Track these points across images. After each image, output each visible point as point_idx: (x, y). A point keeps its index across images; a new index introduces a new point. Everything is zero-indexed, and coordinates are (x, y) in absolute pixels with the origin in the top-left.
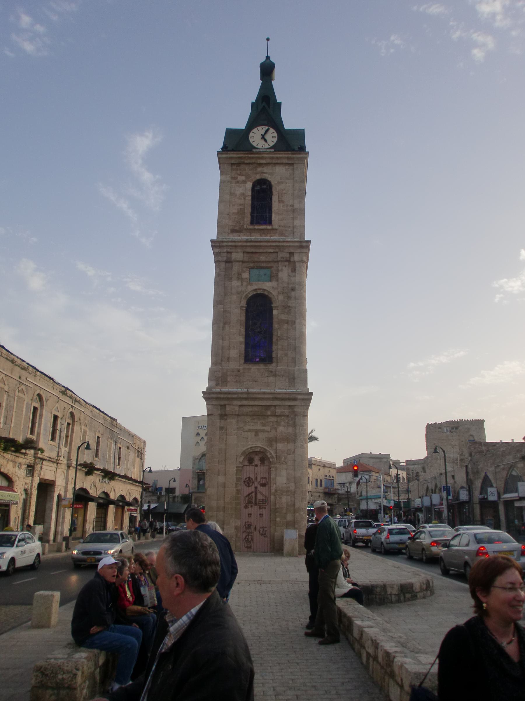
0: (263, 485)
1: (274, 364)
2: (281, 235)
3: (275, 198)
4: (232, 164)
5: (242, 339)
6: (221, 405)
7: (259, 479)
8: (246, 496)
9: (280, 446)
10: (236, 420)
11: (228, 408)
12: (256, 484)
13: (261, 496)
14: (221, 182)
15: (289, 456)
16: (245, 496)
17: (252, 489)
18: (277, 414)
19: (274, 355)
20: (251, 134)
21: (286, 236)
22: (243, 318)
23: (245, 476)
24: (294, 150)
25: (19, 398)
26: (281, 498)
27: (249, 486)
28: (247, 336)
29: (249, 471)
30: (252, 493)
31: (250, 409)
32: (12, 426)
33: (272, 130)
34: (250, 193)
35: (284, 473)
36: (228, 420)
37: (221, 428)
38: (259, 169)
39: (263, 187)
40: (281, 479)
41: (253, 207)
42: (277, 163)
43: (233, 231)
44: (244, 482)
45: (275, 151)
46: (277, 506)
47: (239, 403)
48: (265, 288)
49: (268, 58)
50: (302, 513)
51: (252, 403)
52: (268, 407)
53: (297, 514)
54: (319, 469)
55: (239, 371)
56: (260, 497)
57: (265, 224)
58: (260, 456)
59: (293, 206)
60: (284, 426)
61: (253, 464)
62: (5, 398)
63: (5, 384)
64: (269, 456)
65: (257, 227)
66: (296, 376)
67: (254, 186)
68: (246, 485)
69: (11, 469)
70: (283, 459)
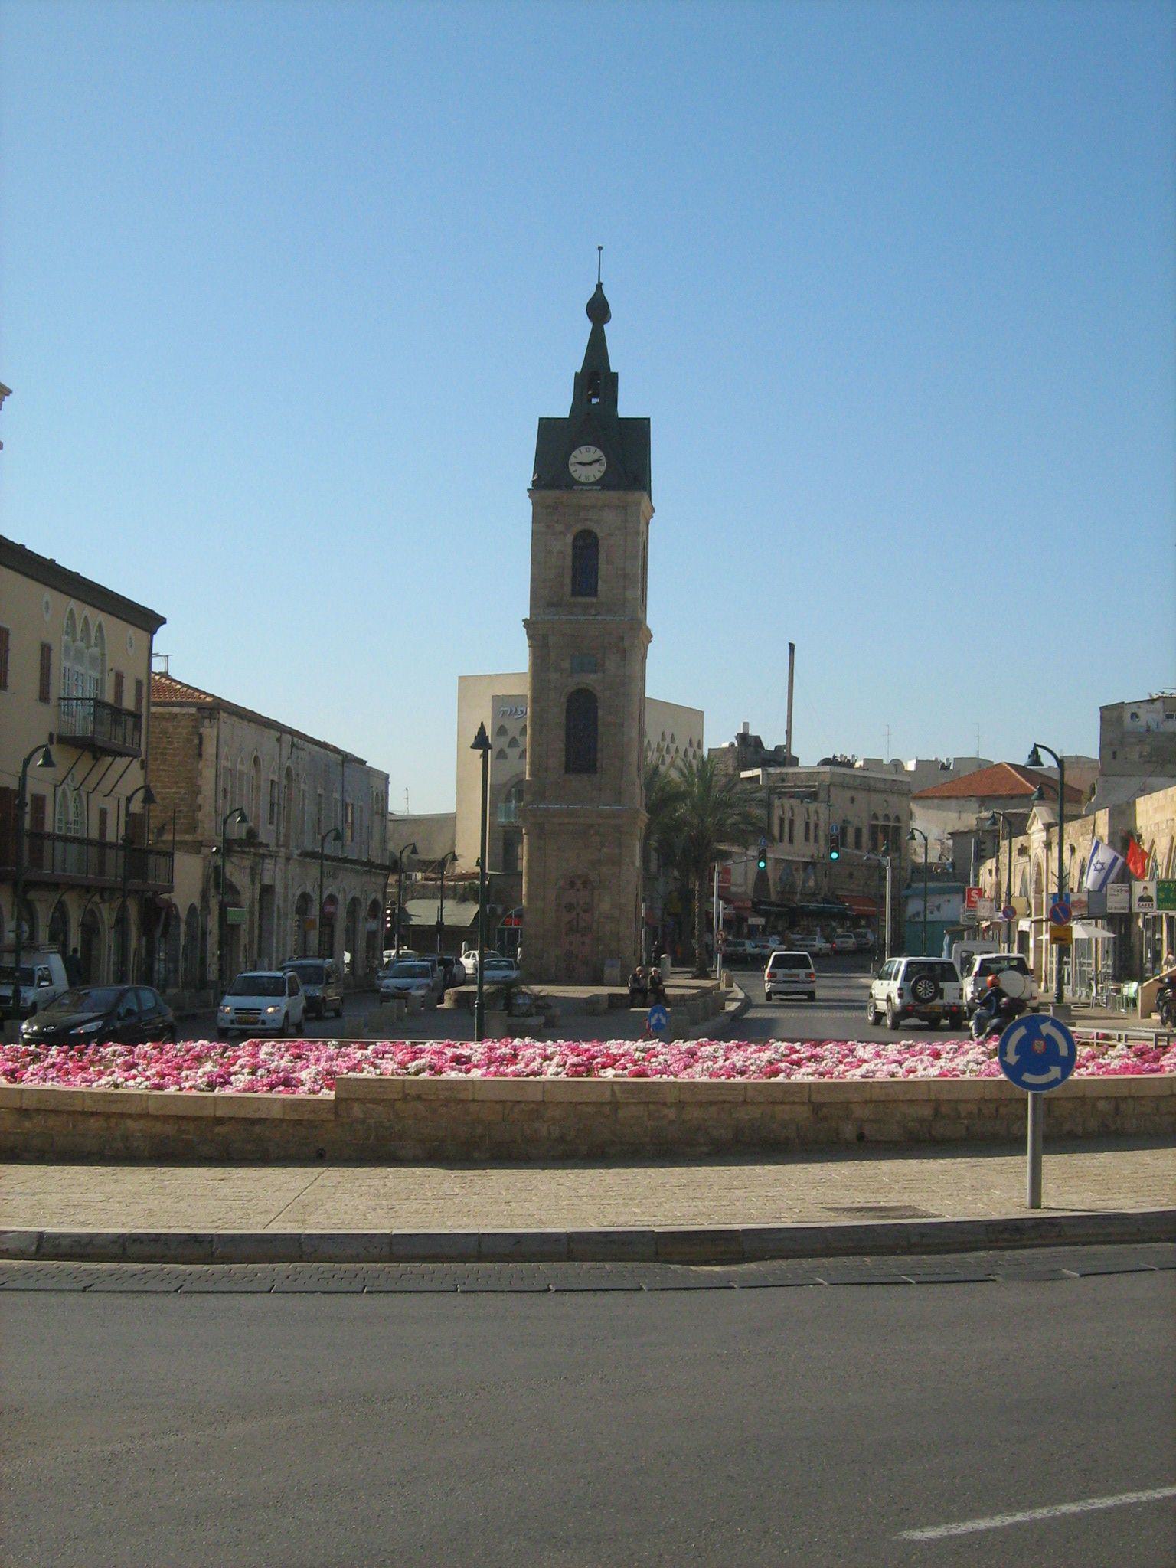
0: (585, 911)
4: (548, 507)
5: (562, 746)
14: (534, 533)
17: (573, 915)
20: (572, 460)
22: (563, 720)
34: (569, 550)
40: (605, 906)
43: (550, 605)
45: (603, 489)
49: (599, 286)
52: (592, 826)
54: (853, 800)
56: (582, 924)
57: (589, 595)
59: (624, 569)
65: (581, 599)
67: (575, 540)
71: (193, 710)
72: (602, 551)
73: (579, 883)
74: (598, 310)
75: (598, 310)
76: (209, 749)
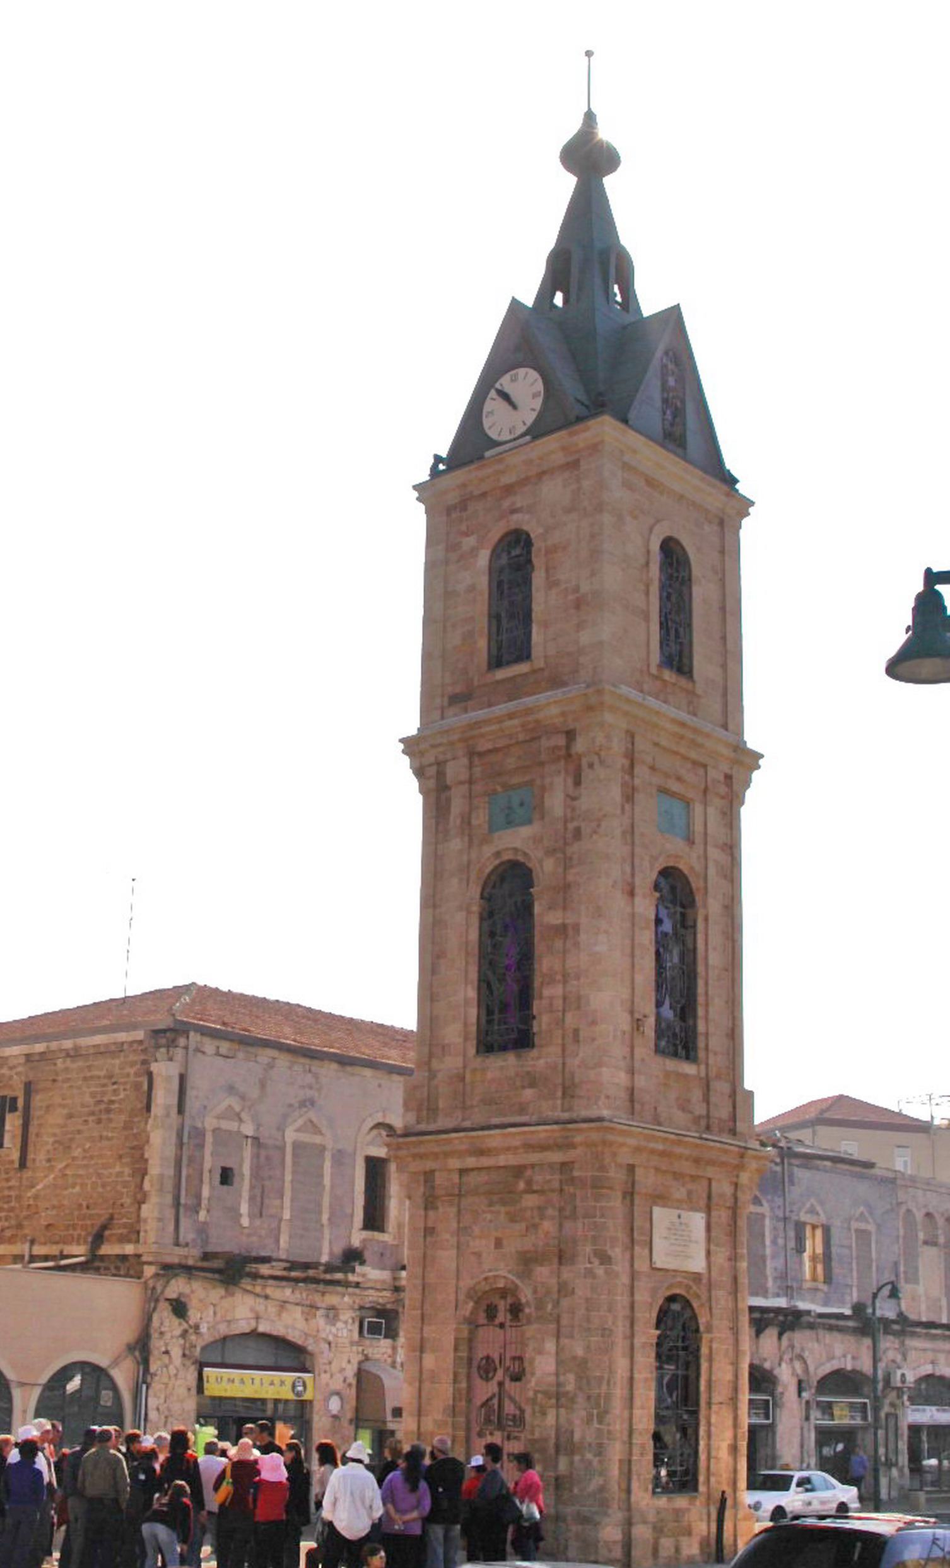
0: (517, 1378)
1: (534, 1053)
2: (556, 682)
3: (538, 578)
5: (472, 994)
6: (425, 1173)
7: (508, 1364)
8: (483, 1405)
9: (543, 1273)
10: (454, 1210)
11: (439, 1179)
12: (500, 1373)
13: (512, 1406)
14: (432, 567)
15: (565, 1303)
16: (479, 1403)
17: (493, 1387)
18: (535, 1188)
19: (535, 1029)
21: (564, 684)
22: (474, 935)
23: (480, 1354)
24: (579, 419)
25: (297, 1146)
26: (544, 1414)
27: (487, 1380)
28: (485, 985)
29: (490, 1342)
30: (494, 1395)
31: (483, 1177)
32: (287, 1215)
33: (533, 375)
35: (550, 1346)
36: (441, 1210)
37: (429, 1231)
38: (506, 504)
39: (513, 553)
40: (543, 1366)
41: (495, 617)
42: (544, 473)
43: (454, 699)
44: (479, 1367)
45: (535, 438)
46: (537, 1435)
47: (455, 1163)
48: (518, 844)
49: (590, 118)
50: (589, 1456)
51: (485, 1161)
52: (518, 1171)
53: (577, 1458)
55: (463, 1079)
58: (509, 1300)
59: (577, 589)
60: (553, 1218)
61: (497, 1321)
62: (248, 1152)
63: (241, 1120)
64: (523, 1300)
65: (501, 674)
66: (577, 1080)
67: (495, 555)
68: (481, 1377)
69: (301, 1324)
70: (550, 1306)
71: (140, 1035)
72: (538, 560)
73: (502, 1305)
74: (589, 158)
75: (589, 158)
76: (164, 1097)
